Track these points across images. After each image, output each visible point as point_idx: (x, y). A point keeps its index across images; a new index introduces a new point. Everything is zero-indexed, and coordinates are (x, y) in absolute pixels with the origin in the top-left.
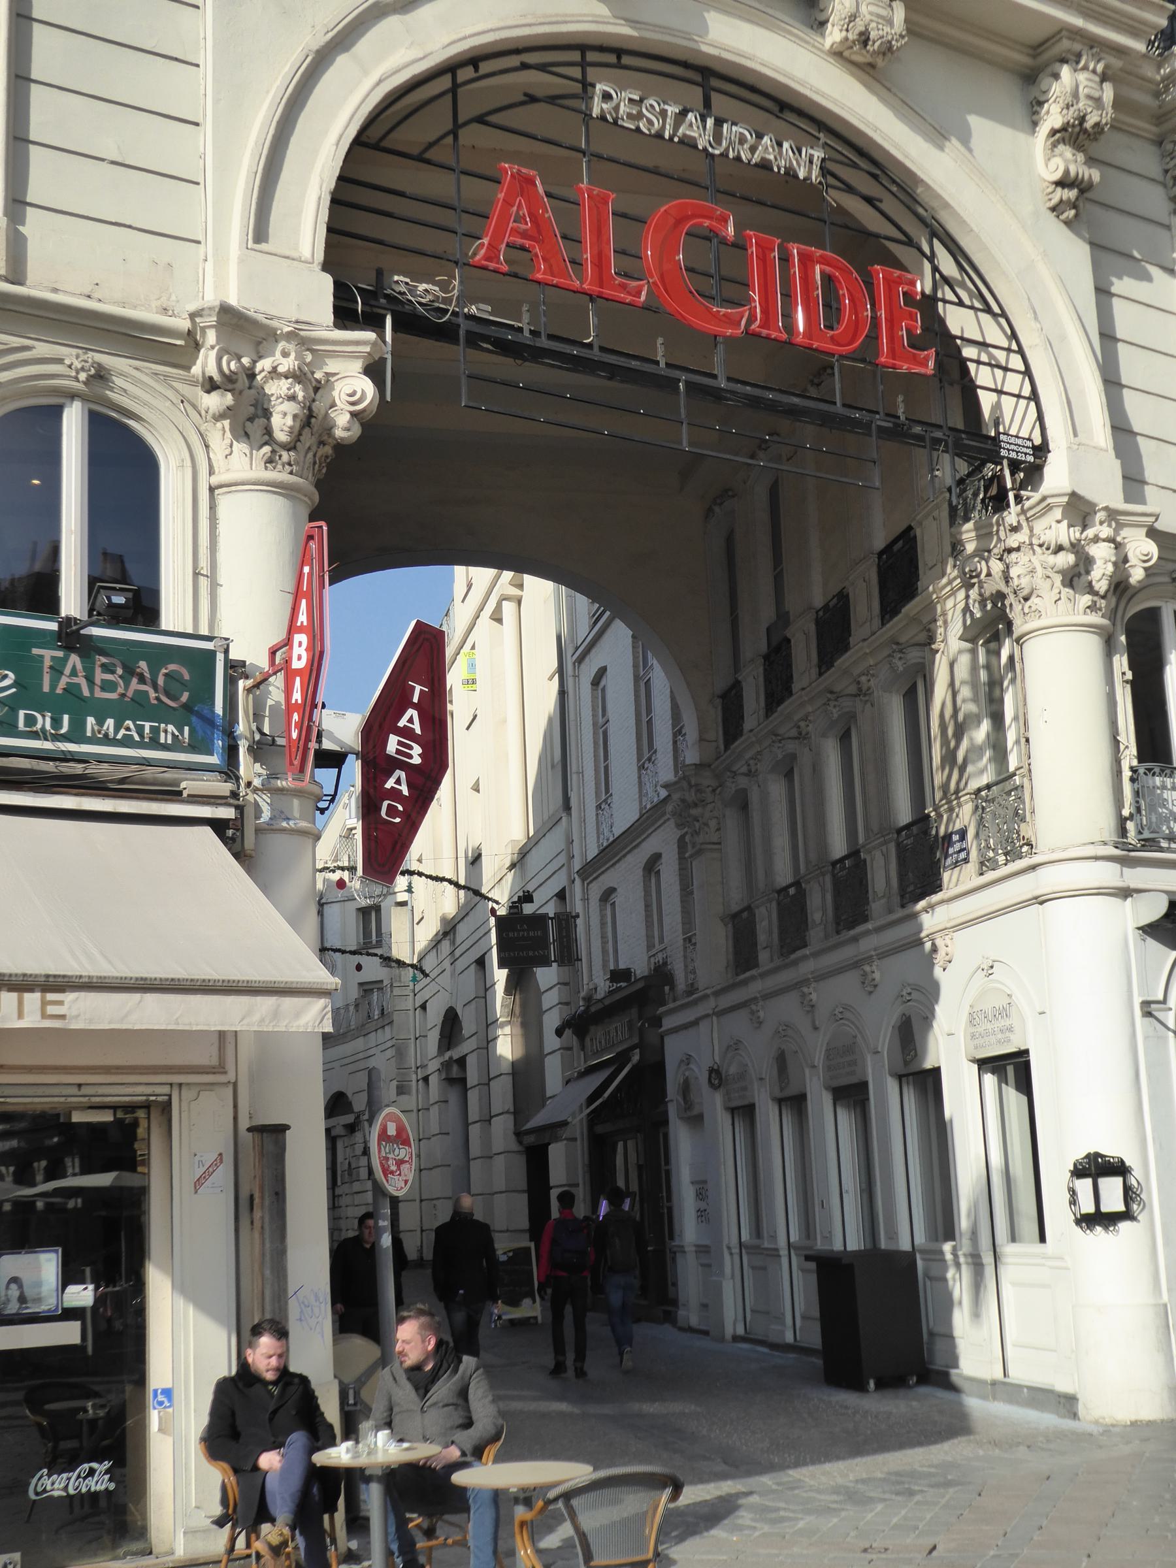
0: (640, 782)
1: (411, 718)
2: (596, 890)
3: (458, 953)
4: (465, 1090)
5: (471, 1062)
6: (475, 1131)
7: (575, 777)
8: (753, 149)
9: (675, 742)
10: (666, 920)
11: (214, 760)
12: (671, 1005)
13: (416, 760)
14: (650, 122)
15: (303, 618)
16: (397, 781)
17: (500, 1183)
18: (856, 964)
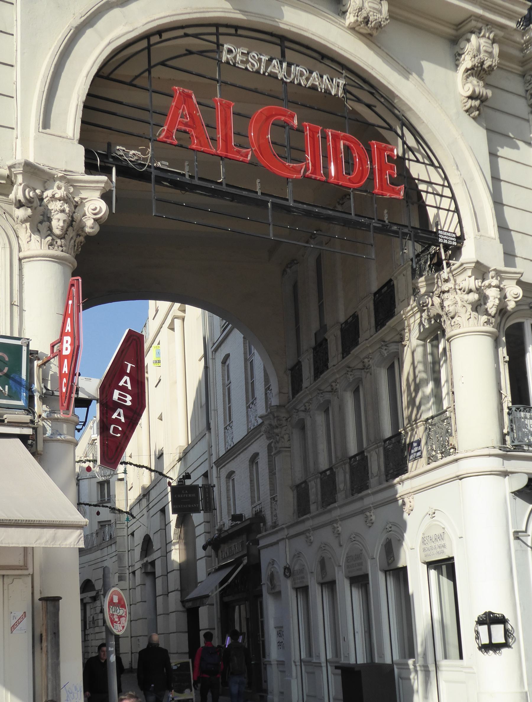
0: (247, 415)
1: (126, 381)
2: (224, 472)
3: (151, 506)
4: (155, 578)
5: (158, 564)
6: (160, 600)
7: (213, 412)
8: (307, 79)
9: (266, 394)
10: (261, 488)
11: (21, 403)
12: (264, 533)
13: (129, 403)
14: (253, 65)
15: (68, 328)
16: (119, 415)
17: (173, 627)
18: (362, 512)
